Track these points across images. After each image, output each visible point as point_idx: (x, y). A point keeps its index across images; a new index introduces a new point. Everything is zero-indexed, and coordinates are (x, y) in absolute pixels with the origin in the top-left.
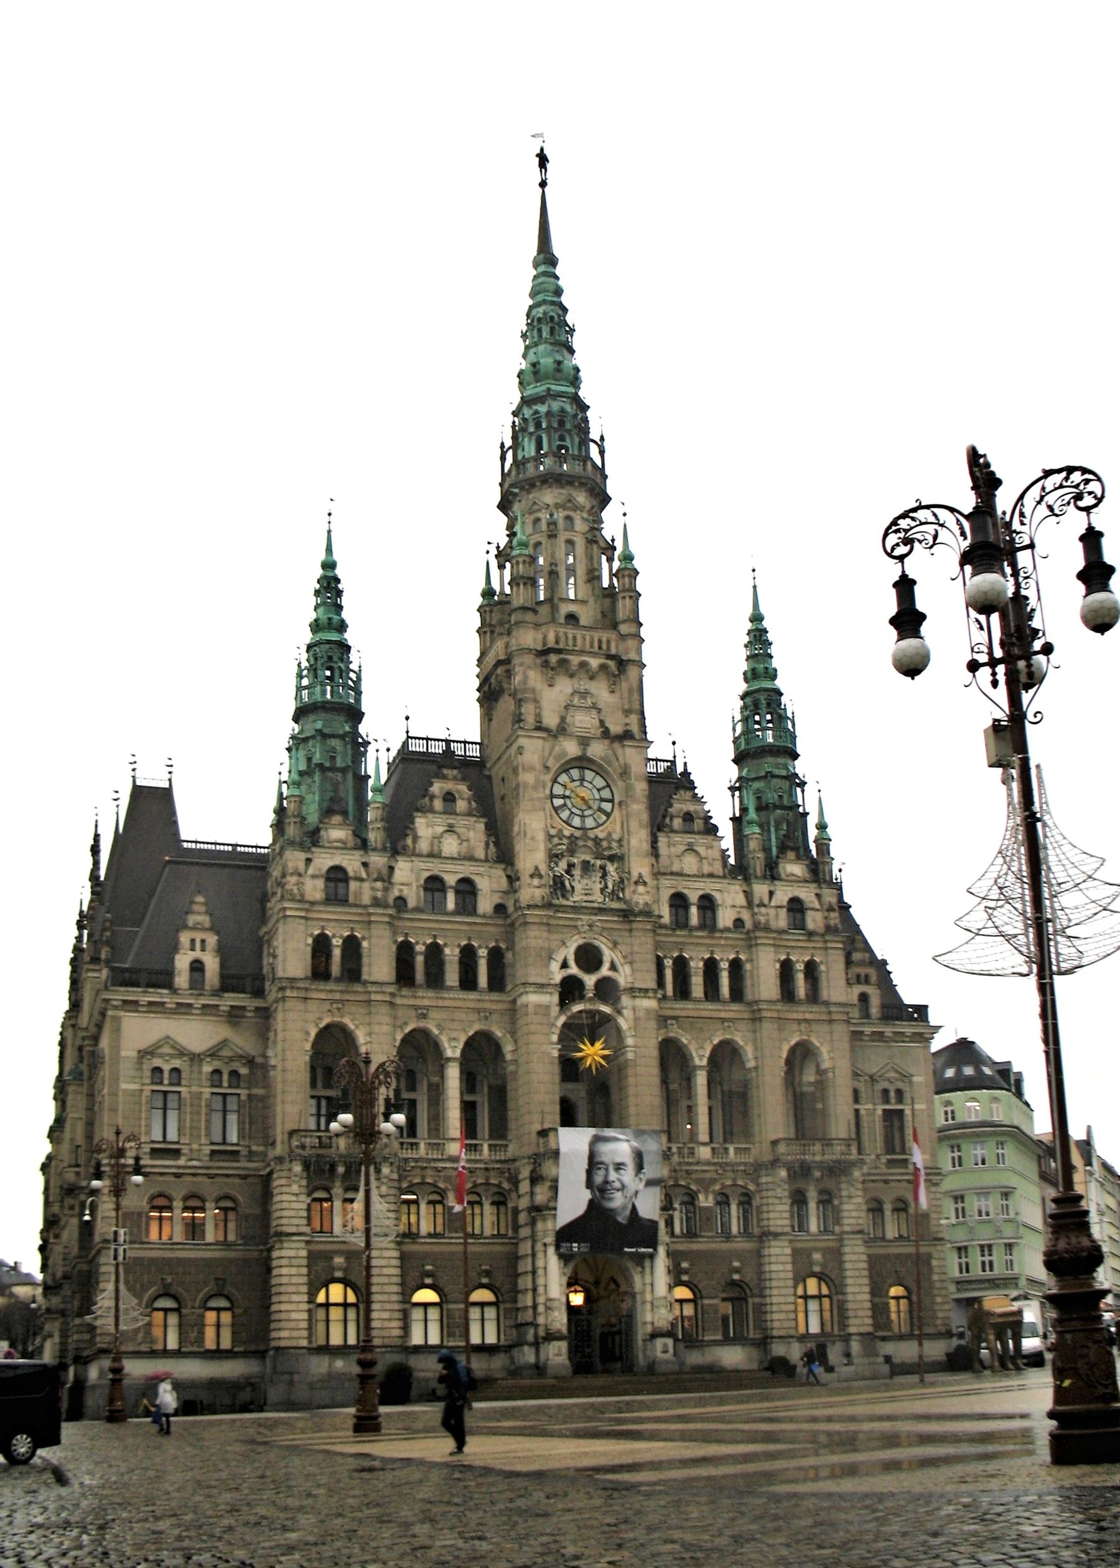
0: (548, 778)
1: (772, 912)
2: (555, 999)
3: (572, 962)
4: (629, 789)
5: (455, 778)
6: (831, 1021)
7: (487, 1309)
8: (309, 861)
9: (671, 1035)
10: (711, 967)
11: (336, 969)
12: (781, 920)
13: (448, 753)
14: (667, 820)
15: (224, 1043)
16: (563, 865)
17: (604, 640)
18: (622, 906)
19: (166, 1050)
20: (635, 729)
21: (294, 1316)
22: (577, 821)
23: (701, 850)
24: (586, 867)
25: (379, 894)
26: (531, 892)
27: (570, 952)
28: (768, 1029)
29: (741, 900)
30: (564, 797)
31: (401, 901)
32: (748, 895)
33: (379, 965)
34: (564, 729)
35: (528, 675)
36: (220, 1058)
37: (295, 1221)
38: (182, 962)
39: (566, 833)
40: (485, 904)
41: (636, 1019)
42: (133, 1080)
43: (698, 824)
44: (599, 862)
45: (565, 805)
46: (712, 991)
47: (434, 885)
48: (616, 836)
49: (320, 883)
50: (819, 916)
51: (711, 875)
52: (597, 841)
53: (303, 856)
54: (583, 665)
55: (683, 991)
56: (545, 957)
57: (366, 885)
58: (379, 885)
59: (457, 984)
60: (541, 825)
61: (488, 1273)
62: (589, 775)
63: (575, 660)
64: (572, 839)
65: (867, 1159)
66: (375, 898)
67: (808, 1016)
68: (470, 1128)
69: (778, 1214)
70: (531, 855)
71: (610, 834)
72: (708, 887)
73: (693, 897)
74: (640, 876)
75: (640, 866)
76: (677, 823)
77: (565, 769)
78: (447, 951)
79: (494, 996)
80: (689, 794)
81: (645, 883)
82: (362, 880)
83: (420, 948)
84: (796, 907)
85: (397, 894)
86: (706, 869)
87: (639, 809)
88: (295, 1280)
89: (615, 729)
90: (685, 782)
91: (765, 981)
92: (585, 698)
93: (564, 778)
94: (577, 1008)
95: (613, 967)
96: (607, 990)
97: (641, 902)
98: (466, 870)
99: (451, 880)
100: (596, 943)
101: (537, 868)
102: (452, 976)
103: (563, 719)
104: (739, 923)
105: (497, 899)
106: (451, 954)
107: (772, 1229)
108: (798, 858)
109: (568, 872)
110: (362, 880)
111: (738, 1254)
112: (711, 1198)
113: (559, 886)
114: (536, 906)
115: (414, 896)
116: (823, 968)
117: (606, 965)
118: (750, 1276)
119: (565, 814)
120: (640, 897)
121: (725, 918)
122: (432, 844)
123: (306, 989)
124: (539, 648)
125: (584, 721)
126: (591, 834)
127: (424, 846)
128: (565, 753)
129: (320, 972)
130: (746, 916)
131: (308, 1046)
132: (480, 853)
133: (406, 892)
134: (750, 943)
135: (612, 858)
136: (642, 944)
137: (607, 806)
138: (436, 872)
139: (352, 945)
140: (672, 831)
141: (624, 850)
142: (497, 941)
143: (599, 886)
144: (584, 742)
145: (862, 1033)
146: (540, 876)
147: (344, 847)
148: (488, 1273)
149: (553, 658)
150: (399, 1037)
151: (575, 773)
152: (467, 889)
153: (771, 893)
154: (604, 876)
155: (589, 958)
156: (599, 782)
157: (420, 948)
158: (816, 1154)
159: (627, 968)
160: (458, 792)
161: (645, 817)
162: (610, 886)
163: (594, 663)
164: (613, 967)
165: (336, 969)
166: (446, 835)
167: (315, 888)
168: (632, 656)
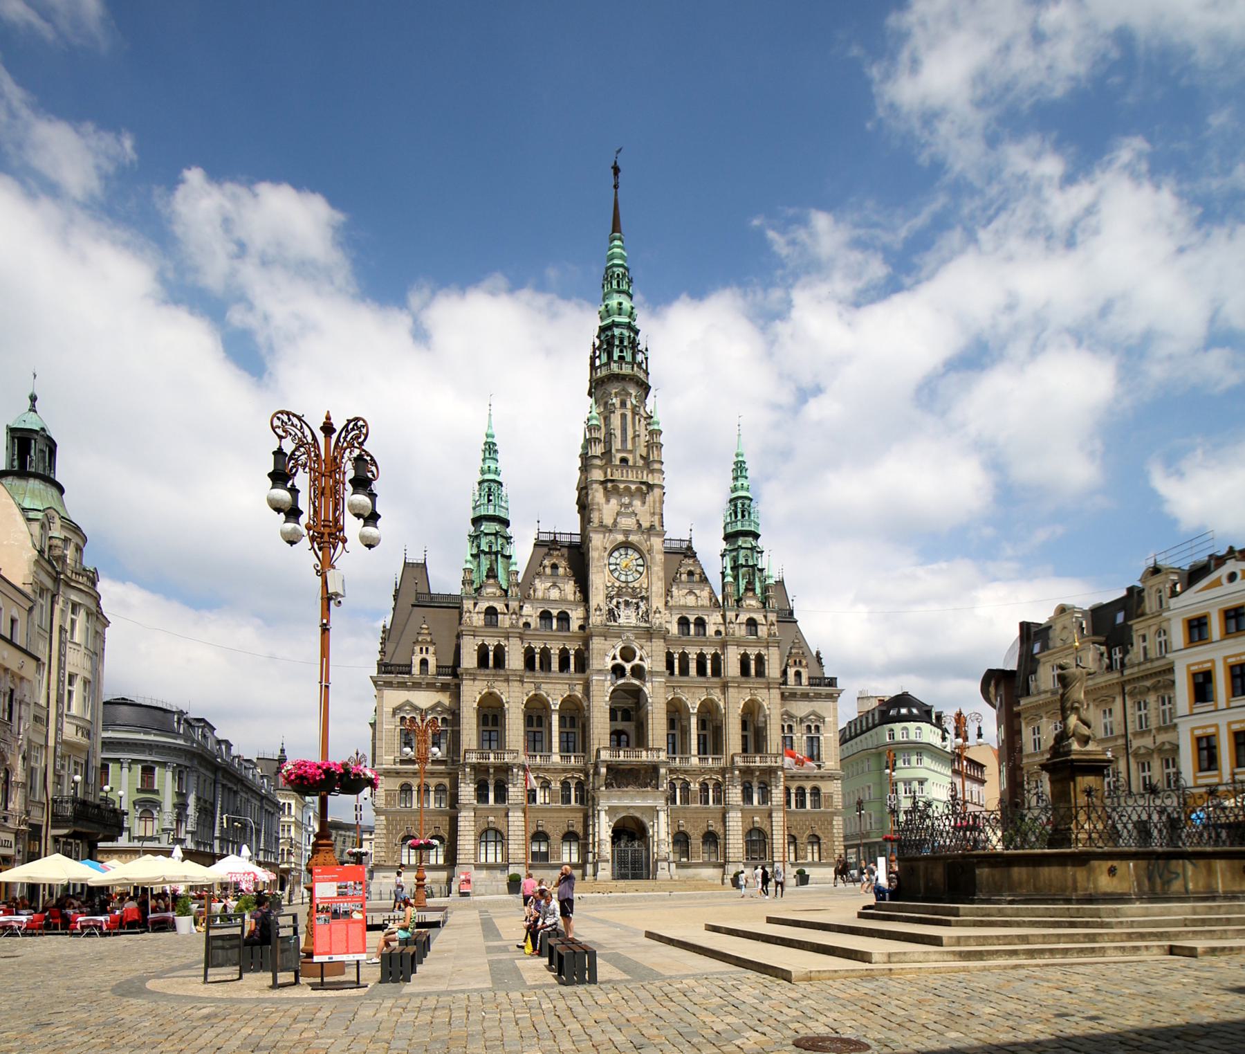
0: (606, 554)
6: (769, 689)
8: (475, 604)
10: (701, 659)
11: (491, 663)
12: (741, 631)
13: (554, 542)
16: (614, 602)
20: (657, 524)
22: (623, 578)
23: (697, 592)
24: (627, 604)
26: (596, 619)
28: (732, 692)
31: (527, 625)
32: (724, 617)
33: (515, 660)
35: (597, 495)
39: (617, 584)
40: (575, 625)
43: (697, 577)
46: (701, 671)
47: (545, 616)
48: (645, 586)
49: (482, 616)
50: (765, 628)
52: (634, 589)
54: (627, 489)
55: (684, 671)
56: (604, 655)
57: (507, 617)
62: (630, 552)
63: (622, 486)
69: (735, 795)
70: (597, 597)
73: (692, 619)
75: (657, 602)
76: (684, 577)
77: (616, 548)
79: (578, 675)
80: (691, 561)
83: (538, 650)
87: (658, 570)
89: (645, 525)
90: (689, 553)
91: (732, 667)
93: (616, 554)
95: (641, 659)
96: (638, 672)
99: (555, 612)
103: (615, 520)
104: (718, 633)
105: (580, 622)
106: (555, 652)
109: (617, 607)
113: (612, 614)
115: (535, 622)
119: (616, 574)
120: (656, 620)
121: (711, 630)
126: (631, 585)
127: (540, 594)
130: (722, 628)
131: (475, 705)
132: (571, 597)
133: (529, 620)
134: (724, 645)
135: (642, 598)
136: (659, 647)
137: (640, 569)
147: (494, 597)
149: (609, 485)
150: (526, 699)
151: (622, 551)
152: (564, 618)
153: (737, 616)
154: (638, 607)
155: (628, 654)
156: (637, 556)
157: (538, 650)
158: (757, 762)
161: (662, 574)
163: (633, 487)
165: (491, 663)
168: (656, 482)
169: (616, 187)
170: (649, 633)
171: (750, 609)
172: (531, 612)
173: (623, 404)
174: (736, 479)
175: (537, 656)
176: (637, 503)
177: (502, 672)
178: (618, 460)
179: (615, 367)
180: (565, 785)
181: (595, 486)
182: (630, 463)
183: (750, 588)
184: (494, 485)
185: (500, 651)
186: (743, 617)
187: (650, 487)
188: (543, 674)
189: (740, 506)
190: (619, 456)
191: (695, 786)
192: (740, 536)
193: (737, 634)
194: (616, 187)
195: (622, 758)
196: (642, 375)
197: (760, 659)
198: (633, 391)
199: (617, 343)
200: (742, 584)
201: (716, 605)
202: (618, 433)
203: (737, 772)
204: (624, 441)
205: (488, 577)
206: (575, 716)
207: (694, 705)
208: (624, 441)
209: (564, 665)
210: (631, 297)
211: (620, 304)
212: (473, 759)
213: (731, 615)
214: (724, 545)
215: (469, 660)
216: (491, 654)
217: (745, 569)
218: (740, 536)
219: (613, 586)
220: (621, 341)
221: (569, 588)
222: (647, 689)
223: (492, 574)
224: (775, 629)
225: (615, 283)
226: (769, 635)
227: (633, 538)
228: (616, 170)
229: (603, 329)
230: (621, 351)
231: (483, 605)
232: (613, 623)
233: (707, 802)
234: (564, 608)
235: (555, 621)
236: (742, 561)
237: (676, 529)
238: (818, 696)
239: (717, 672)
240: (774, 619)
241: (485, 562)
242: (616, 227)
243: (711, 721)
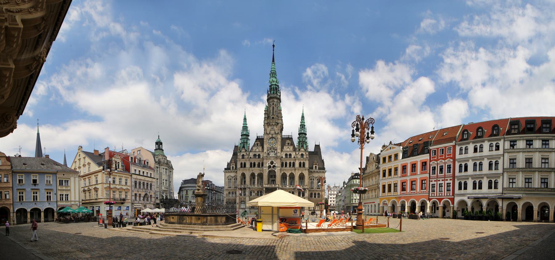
10: (290, 163)
12: (299, 157)
33: (248, 165)
46: (290, 165)
47: (255, 155)
55: (286, 166)
56: (267, 164)
68: (258, 184)
70: (265, 150)
84: (302, 155)
91: (297, 165)
98: (259, 153)
102: (256, 166)
113: (268, 154)
115: (252, 157)
120: (279, 155)
121: (293, 156)
125: (273, 132)
129: (241, 167)
134: (295, 160)
139: (245, 164)
152: (259, 155)
155: (272, 163)
170: (277, 158)
171: (302, 151)
172: (251, 154)
173: (273, 104)
176: (275, 127)
178: (273, 117)
179: (272, 96)
180: (258, 192)
186: (300, 153)
187: (278, 124)
192: (302, 134)
197: (304, 164)
198: (276, 100)
206: (261, 176)
207: (288, 174)
212: (239, 187)
213: (297, 153)
215: (239, 166)
218: (302, 134)
221: (260, 148)
223: (244, 147)
227: (274, 136)
231: (242, 154)
237: (285, 133)
238: (320, 172)
241: (242, 145)
243: (292, 177)
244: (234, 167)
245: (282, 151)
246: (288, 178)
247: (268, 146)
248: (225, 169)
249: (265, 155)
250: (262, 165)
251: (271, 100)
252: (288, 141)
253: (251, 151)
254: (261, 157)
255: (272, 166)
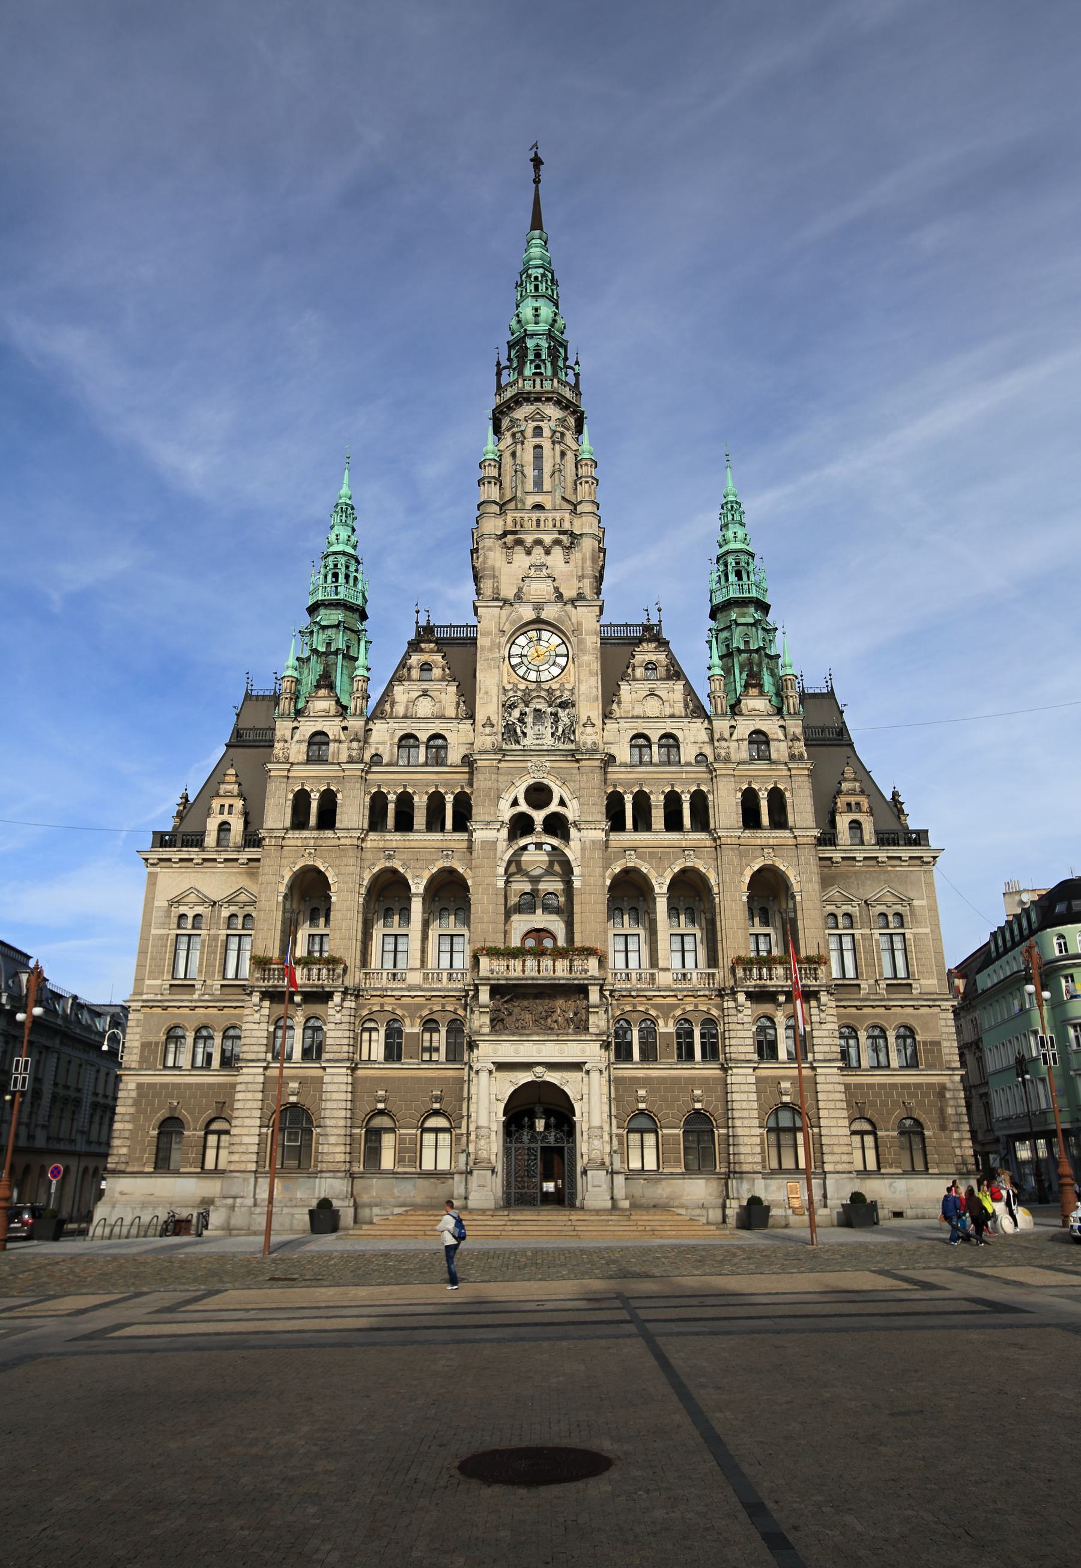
0: (504, 640)
1: (733, 745)
2: (504, 833)
3: (521, 800)
4: (580, 642)
5: (432, 651)
7: (441, 1136)
9: (632, 865)
10: (673, 801)
11: (313, 820)
12: (742, 751)
14: (630, 671)
15: (239, 892)
16: (516, 713)
17: (558, 519)
18: (572, 747)
19: (192, 898)
21: (246, 1140)
22: (533, 676)
25: (354, 753)
27: (520, 791)
28: (728, 856)
29: (704, 736)
30: (522, 656)
31: (377, 759)
32: (711, 731)
33: (352, 812)
34: (520, 598)
35: (494, 556)
36: (236, 904)
37: (255, 1048)
38: (212, 825)
39: (522, 687)
41: (583, 849)
42: (162, 925)
44: (549, 710)
45: (522, 662)
47: (407, 740)
48: (569, 686)
49: (304, 747)
50: (783, 746)
51: (672, 716)
53: (290, 725)
54: (538, 542)
55: (643, 821)
57: (344, 746)
58: (355, 744)
59: (424, 827)
60: (496, 680)
61: (439, 1099)
62: (545, 635)
63: (529, 539)
64: (527, 692)
65: (864, 985)
66: (350, 756)
67: (771, 842)
70: (488, 707)
71: (562, 685)
72: (669, 727)
74: (589, 718)
78: (416, 798)
81: (593, 725)
82: (340, 742)
83: (392, 797)
85: (373, 752)
86: (668, 711)
87: (591, 660)
88: (249, 1105)
89: (569, 593)
91: (726, 809)
92: (541, 570)
93: (522, 640)
94: (522, 842)
95: (562, 803)
96: (557, 826)
97: (589, 742)
99: (423, 736)
100: (545, 781)
101: (489, 718)
102: (420, 819)
103: (520, 590)
104: (701, 758)
105: (463, 751)
107: (733, 1056)
108: (762, 693)
109: (521, 720)
110: (340, 742)
111: (703, 1082)
112: (671, 1022)
114: (486, 752)
116: (788, 794)
117: (556, 800)
118: (715, 1108)
119: (521, 671)
120: (587, 737)
121: (688, 753)
122: (407, 708)
123: (283, 838)
124: (499, 533)
125: (540, 589)
127: (400, 710)
128: (521, 618)
129: (299, 821)
130: (708, 750)
132: (451, 712)
135: (564, 705)
137: (562, 661)
138: (409, 731)
140: (634, 680)
141: (574, 698)
142: (462, 787)
143: (550, 731)
144: (538, 607)
145: (854, 858)
146: (493, 726)
147: (326, 715)
148: (439, 1099)
155: (539, 795)
157: (392, 797)
159: (575, 801)
160: (433, 661)
161: (596, 666)
162: (560, 730)
163: (548, 539)
164: (562, 803)
165: (313, 820)
166: (421, 699)
167: (299, 752)
169: (537, 181)
171: (754, 714)
173: (538, 432)
174: (725, 526)
175: (391, 807)
177: (329, 833)
179: (528, 387)
181: (488, 542)
182: (548, 506)
183: (753, 681)
184: (342, 560)
185: (329, 802)
188: (398, 836)
189: (734, 564)
190: (530, 500)
191: (666, 1027)
193: (734, 757)
194: (537, 181)
195: (518, 973)
196: (567, 393)
197: (777, 798)
198: (552, 411)
199: (531, 357)
200: (740, 678)
201: (697, 711)
202: (530, 472)
203: (741, 997)
204: (538, 482)
205: (318, 687)
208: (538, 482)
209: (435, 822)
210: (557, 306)
211: (536, 309)
214: (712, 624)
215: (277, 813)
216: (314, 805)
217: (744, 656)
219: (515, 689)
220: (538, 355)
222: (572, 852)
223: (325, 681)
224: (800, 747)
225: (531, 287)
226: (792, 757)
227: (550, 613)
228: (537, 162)
229: (511, 346)
230: (538, 367)
232: (514, 747)
233: (690, 1056)
234: (437, 727)
235: (422, 749)
236: (738, 643)
239: (701, 821)
240: (799, 731)
241: (317, 666)
242: (537, 223)
244: (237, 825)
245: (607, 715)
246: (662, 905)
247: (507, 678)
248: (162, 840)
249: (486, 740)
250: (462, 822)
251: (523, 411)
252: (646, 653)
253: (378, 714)
254: (454, 756)
255: (539, 818)
